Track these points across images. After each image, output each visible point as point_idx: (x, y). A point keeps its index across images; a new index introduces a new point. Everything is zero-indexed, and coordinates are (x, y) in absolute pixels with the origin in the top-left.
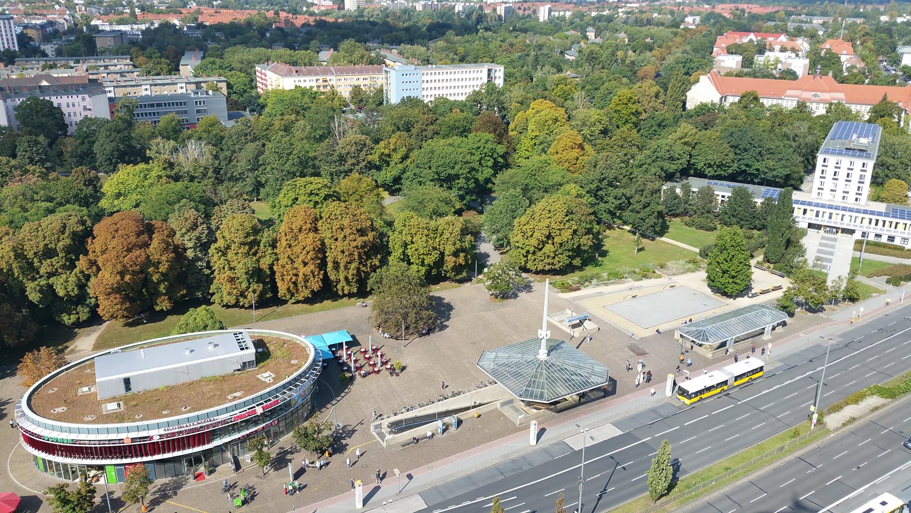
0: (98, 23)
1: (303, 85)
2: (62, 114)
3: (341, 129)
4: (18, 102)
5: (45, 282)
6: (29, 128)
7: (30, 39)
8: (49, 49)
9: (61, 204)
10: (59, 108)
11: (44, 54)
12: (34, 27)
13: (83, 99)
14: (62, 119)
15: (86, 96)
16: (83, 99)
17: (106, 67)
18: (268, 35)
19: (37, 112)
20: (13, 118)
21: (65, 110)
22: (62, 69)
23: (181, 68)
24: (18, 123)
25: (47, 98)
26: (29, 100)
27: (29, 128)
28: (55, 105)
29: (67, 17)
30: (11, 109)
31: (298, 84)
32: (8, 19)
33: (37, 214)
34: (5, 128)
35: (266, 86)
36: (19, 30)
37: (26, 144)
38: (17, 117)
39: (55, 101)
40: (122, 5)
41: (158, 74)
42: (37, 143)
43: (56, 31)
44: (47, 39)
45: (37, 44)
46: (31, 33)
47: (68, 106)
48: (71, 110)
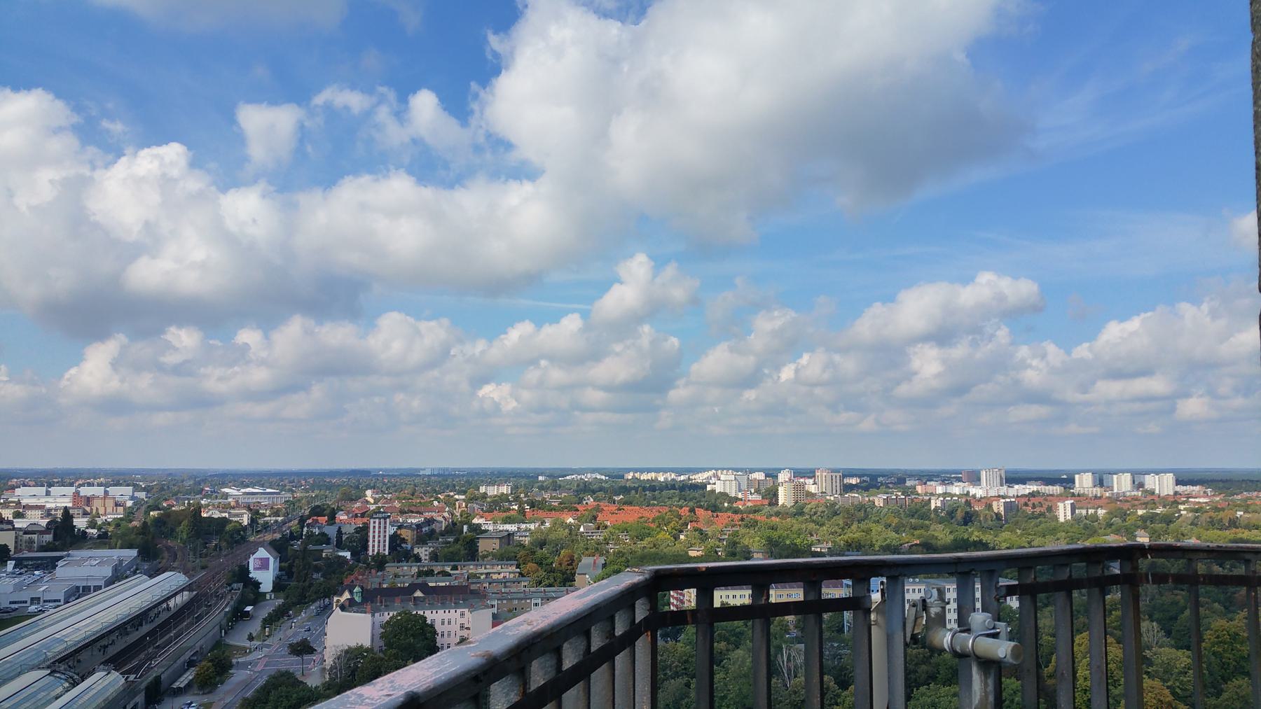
0: (481, 521)
1: (732, 602)
2: (435, 633)
3: (792, 665)
4: (387, 617)
6: (394, 651)
7: (404, 541)
8: (423, 552)
10: (432, 626)
11: (418, 559)
12: (410, 527)
13: (462, 614)
14: (435, 641)
15: (466, 611)
16: (462, 614)
17: (487, 574)
18: (682, 537)
19: (407, 630)
20: (377, 637)
21: (439, 628)
22: (440, 577)
23: (577, 577)
24: (382, 643)
25: (421, 612)
26: (399, 614)
27: (394, 651)
28: (429, 622)
29: (446, 515)
30: (377, 625)
31: (725, 600)
32: (385, 518)
34: (367, 650)
35: (682, 602)
36: (391, 530)
38: (382, 636)
39: (430, 616)
40: (509, 501)
41: (550, 585)
43: (433, 531)
44: (421, 540)
45: (409, 546)
46: (406, 534)
47: (443, 623)
48: (446, 628)
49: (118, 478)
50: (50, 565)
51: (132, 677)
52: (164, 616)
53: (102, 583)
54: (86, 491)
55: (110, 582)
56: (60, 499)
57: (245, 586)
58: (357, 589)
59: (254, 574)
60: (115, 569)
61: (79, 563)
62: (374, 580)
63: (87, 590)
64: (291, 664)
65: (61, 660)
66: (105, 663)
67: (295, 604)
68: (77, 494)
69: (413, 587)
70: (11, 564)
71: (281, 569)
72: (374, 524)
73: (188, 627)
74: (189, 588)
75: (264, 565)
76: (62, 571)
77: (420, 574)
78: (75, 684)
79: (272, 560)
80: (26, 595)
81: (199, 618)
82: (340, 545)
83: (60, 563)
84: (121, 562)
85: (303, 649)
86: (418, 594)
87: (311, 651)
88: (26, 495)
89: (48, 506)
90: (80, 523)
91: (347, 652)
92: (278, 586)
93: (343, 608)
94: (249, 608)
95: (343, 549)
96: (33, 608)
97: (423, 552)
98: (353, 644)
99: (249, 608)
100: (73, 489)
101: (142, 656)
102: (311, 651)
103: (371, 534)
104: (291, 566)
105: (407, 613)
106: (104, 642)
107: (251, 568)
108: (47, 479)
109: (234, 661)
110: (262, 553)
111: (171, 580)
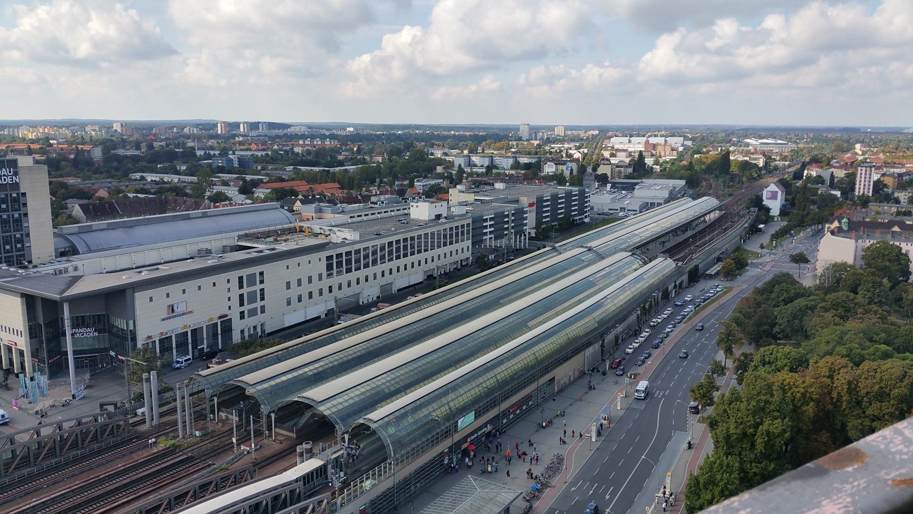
4: (868, 243)
5: (868, 423)
6: (873, 270)
7: (886, 186)
8: (903, 196)
9: (898, 350)
11: (897, 201)
12: (892, 175)
19: (884, 255)
20: (859, 258)
24: (862, 263)
25: (897, 244)
26: (878, 243)
27: (873, 270)
28: (904, 251)
30: (860, 249)
32: (871, 167)
33: (874, 354)
34: (850, 266)
36: (875, 177)
37: (871, 285)
38: (863, 257)
39: (905, 247)
42: (880, 284)
44: (902, 186)
45: (890, 191)
46: (888, 181)
49: (674, 132)
50: (631, 188)
51: (680, 264)
52: (702, 226)
53: (662, 201)
54: (653, 140)
55: (667, 201)
56: (637, 145)
57: (759, 210)
58: (845, 220)
59: (766, 202)
60: (671, 193)
61: (649, 187)
62: (858, 215)
63: (653, 205)
64: (792, 269)
65: (638, 248)
66: (664, 252)
67: (795, 226)
68: (647, 142)
69: (891, 224)
70: (609, 186)
71: (786, 200)
72: (861, 171)
73: (718, 235)
74: (719, 208)
75: (774, 196)
76: (638, 192)
77: (899, 213)
78: (645, 263)
79: (780, 193)
80: (617, 206)
81: (726, 229)
82: (832, 186)
83: (637, 187)
84: (674, 188)
85: (800, 259)
86: (896, 229)
87: (807, 261)
88: (618, 142)
89: (630, 150)
90: (649, 161)
91: (834, 265)
92: (783, 213)
93: (833, 233)
94: (761, 226)
95: (835, 189)
96: (621, 214)
97: (903, 196)
98: (839, 260)
99: (761, 226)
100: (644, 139)
101: (687, 251)
102: (807, 261)
103: (858, 179)
104: (793, 199)
105: (886, 243)
106: (663, 239)
107: (764, 198)
108: (630, 132)
109: (749, 261)
110: (773, 187)
111: (707, 203)
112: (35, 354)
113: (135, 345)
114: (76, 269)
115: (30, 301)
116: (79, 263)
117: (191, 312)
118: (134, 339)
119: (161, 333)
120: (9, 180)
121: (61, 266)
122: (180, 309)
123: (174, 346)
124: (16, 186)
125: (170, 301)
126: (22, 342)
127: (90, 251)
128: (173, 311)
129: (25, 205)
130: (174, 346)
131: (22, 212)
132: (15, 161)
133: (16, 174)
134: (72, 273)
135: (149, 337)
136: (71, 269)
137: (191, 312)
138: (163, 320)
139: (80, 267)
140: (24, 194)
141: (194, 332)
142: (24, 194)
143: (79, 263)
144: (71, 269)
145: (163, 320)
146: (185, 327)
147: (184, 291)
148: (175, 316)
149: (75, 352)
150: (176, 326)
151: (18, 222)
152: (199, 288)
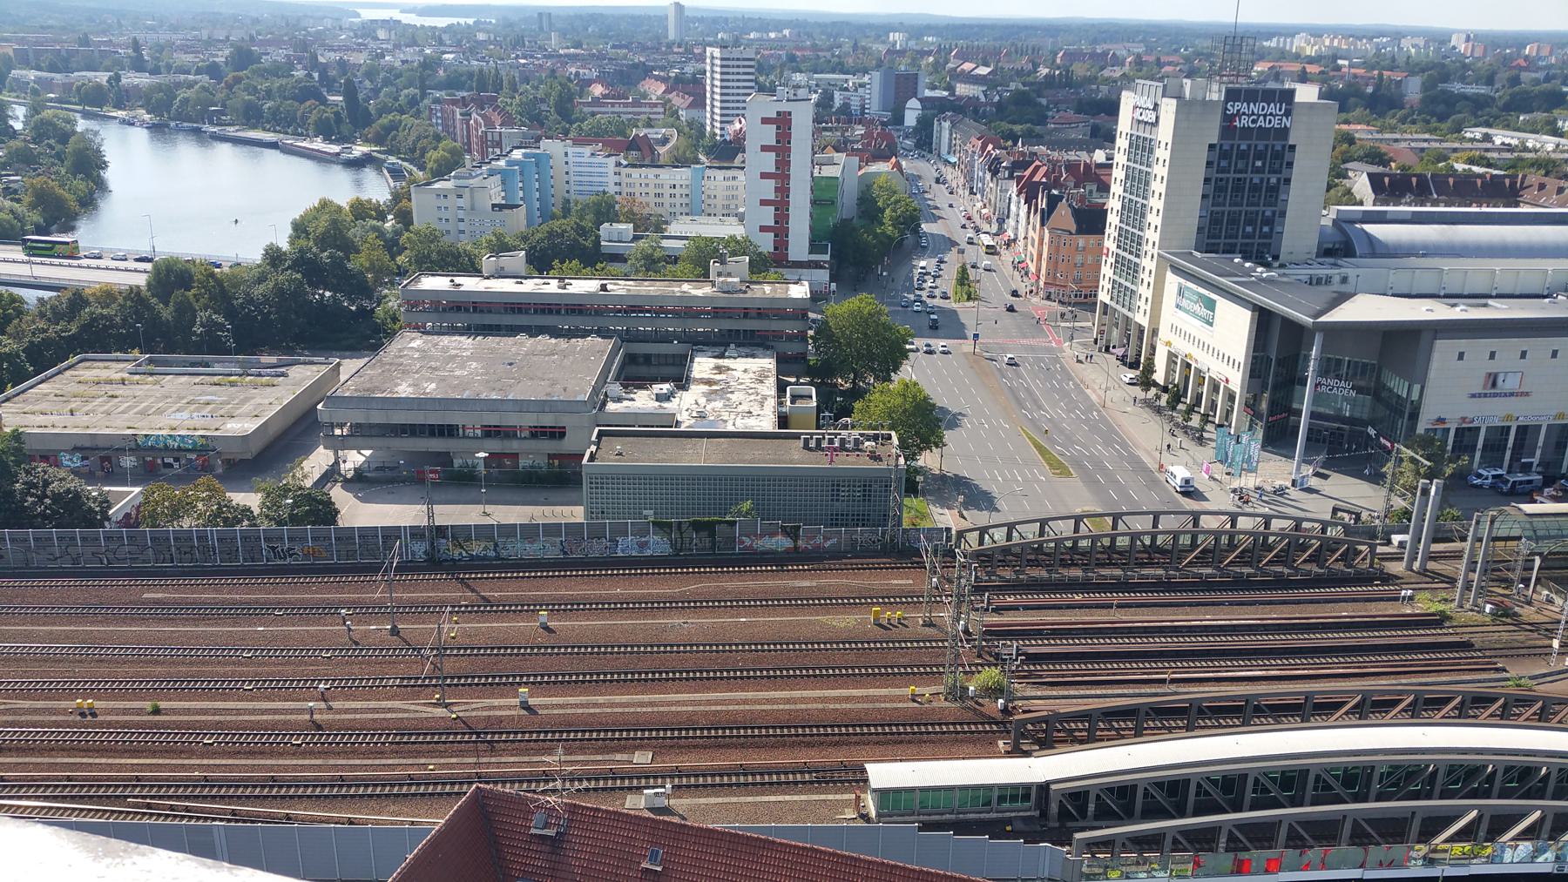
112: (1251, 405)
113: (1413, 427)
114: (1344, 280)
115: (1264, 320)
116: (1351, 272)
117: (1527, 394)
118: (1414, 416)
119: (1464, 419)
120: (1275, 123)
121: (1322, 272)
122: (1510, 384)
123: (1480, 445)
124: (1284, 133)
125: (1492, 367)
126: (1236, 380)
127: (1374, 255)
128: (1494, 385)
129: (1290, 165)
130: (1480, 445)
131: (1283, 176)
132: (1292, 92)
133: (1288, 114)
134: (1336, 286)
135: (1441, 420)
136: (1336, 279)
137: (1527, 394)
138: (1473, 396)
139: (1352, 279)
140: (1293, 148)
141: (1523, 431)
142: (1293, 148)
143: (1351, 272)
144: (1336, 279)
145: (1473, 396)
146: (1509, 417)
147: (1523, 355)
148: (1495, 395)
149: (1313, 415)
150: (1491, 413)
151: (1274, 191)
152: (1555, 354)
